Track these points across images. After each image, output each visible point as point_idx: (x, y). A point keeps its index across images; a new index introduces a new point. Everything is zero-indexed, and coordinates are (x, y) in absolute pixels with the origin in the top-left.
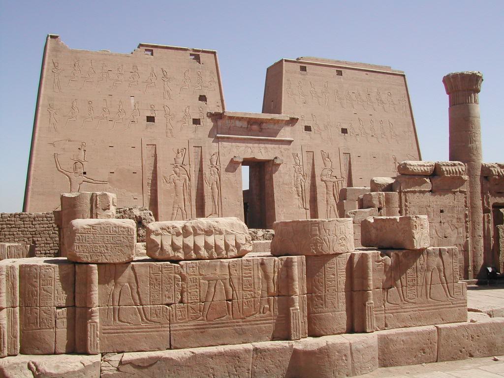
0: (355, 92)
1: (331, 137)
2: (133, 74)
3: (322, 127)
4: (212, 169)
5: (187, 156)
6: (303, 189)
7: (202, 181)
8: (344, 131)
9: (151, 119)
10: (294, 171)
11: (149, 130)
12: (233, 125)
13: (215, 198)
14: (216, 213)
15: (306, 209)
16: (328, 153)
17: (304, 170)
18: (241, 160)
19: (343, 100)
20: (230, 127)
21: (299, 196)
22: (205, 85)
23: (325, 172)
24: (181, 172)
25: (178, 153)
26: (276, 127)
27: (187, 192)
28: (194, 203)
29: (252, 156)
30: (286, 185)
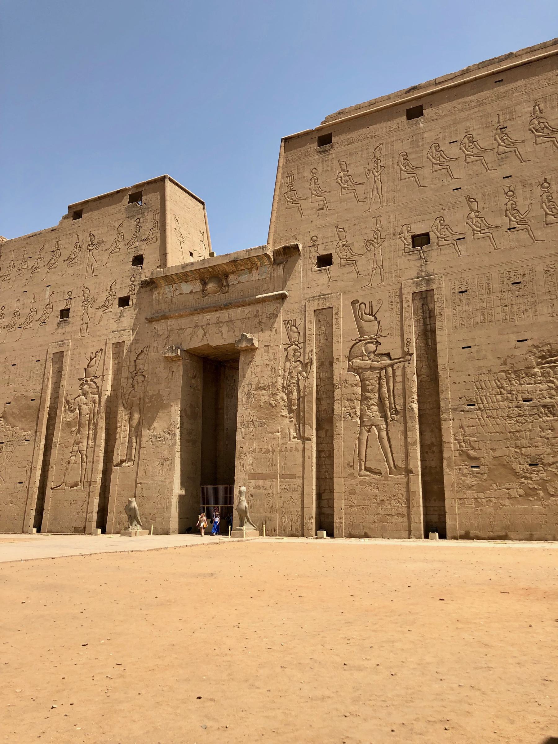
0: (460, 137)
1: (380, 264)
2: (55, 253)
3: (358, 246)
6: (302, 394)
8: (421, 240)
9: (65, 313)
10: (282, 360)
11: (60, 330)
12: (178, 292)
14: (130, 460)
15: (305, 439)
16: (370, 303)
17: (308, 350)
19: (422, 168)
20: (172, 297)
21: (290, 411)
22: (143, 238)
23: (361, 348)
24: (90, 391)
26: (255, 276)
29: (205, 342)
30: (264, 388)
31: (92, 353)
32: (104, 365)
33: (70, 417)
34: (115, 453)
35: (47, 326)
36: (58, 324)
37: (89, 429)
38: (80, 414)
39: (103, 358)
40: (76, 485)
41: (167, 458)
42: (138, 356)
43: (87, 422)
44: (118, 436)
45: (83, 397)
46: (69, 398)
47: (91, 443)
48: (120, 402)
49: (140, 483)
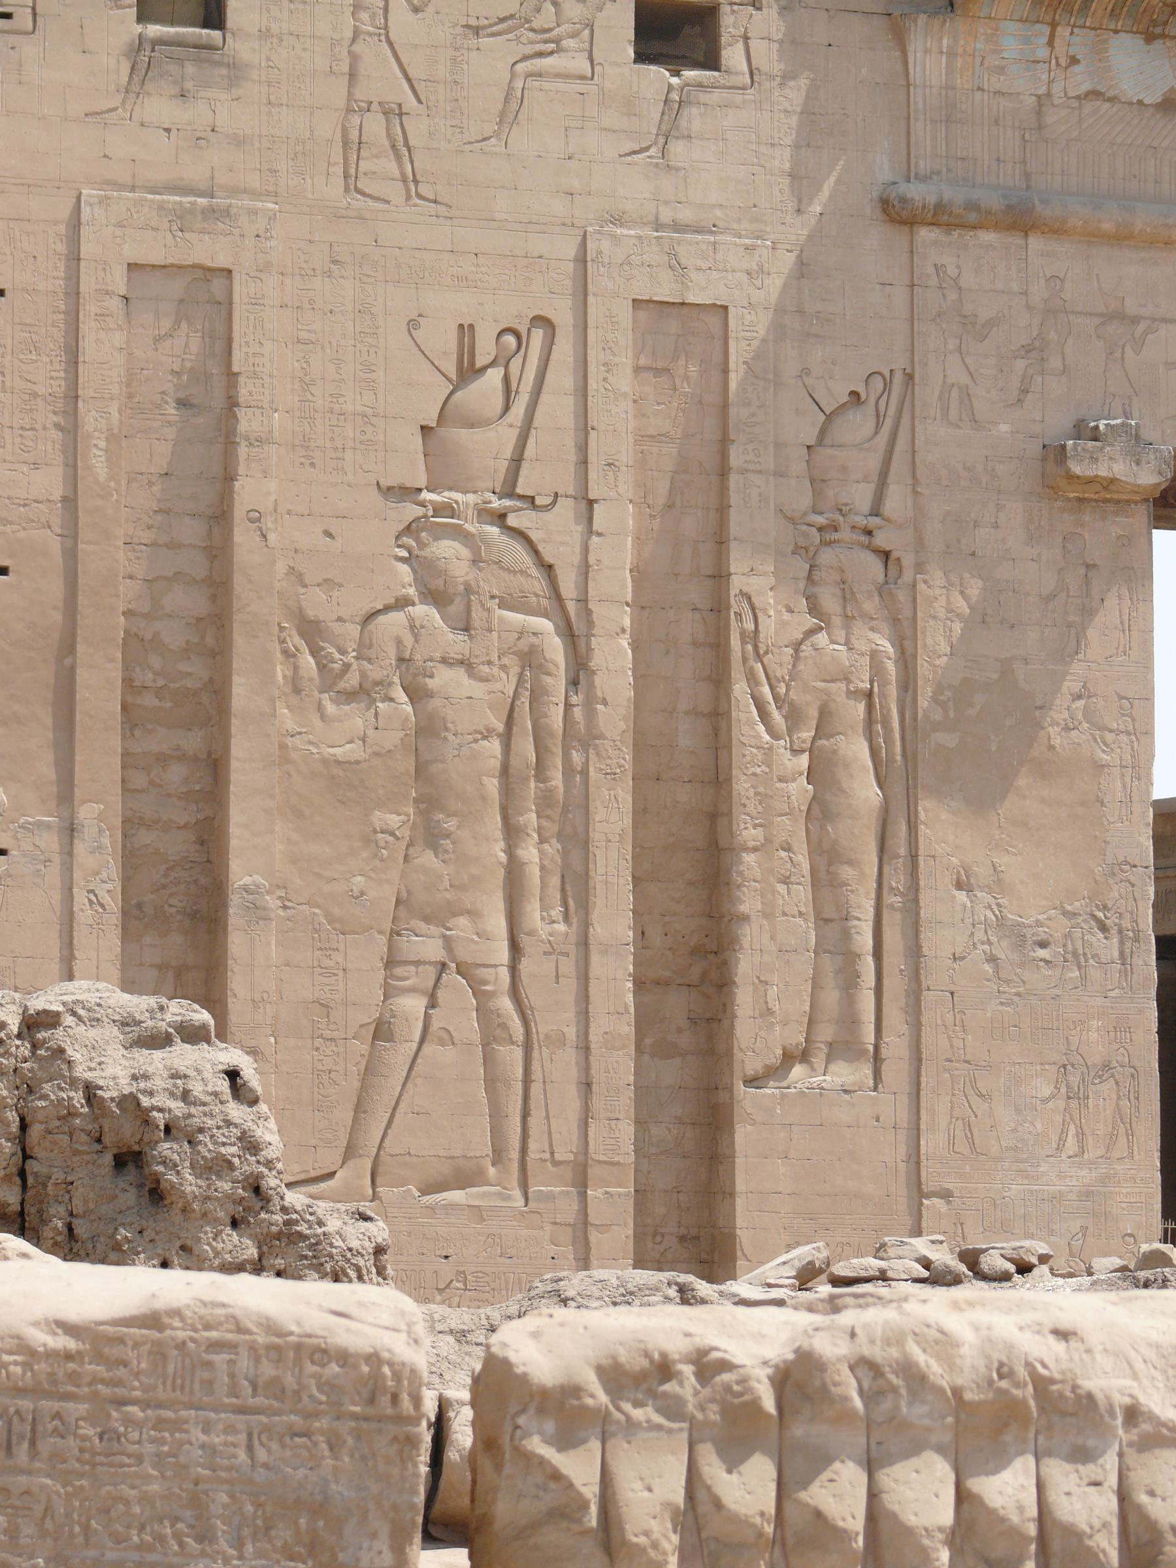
4: (827, 557)
5: (558, 407)
7: (718, 679)
11: (159, 106)
12: (1081, 80)
13: (847, 873)
14: (844, 1048)
18: (1149, 477)
20: (1043, 100)
25: (468, 371)
27: (545, 801)
28: (614, 922)
31: (466, 332)
32: (584, 429)
33: (344, 734)
34: (744, 1000)
35: (29, 49)
36: (143, 61)
37: (512, 833)
38: (428, 728)
39: (561, 377)
40: (464, 1178)
41: (1107, 1066)
42: (829, 418)
43: (492, 785)
44: (748, 903)
45: (423, 611)
46: (316, 603)
47: (544, 921)
48: (740, 689)
49: (946, 1195)
